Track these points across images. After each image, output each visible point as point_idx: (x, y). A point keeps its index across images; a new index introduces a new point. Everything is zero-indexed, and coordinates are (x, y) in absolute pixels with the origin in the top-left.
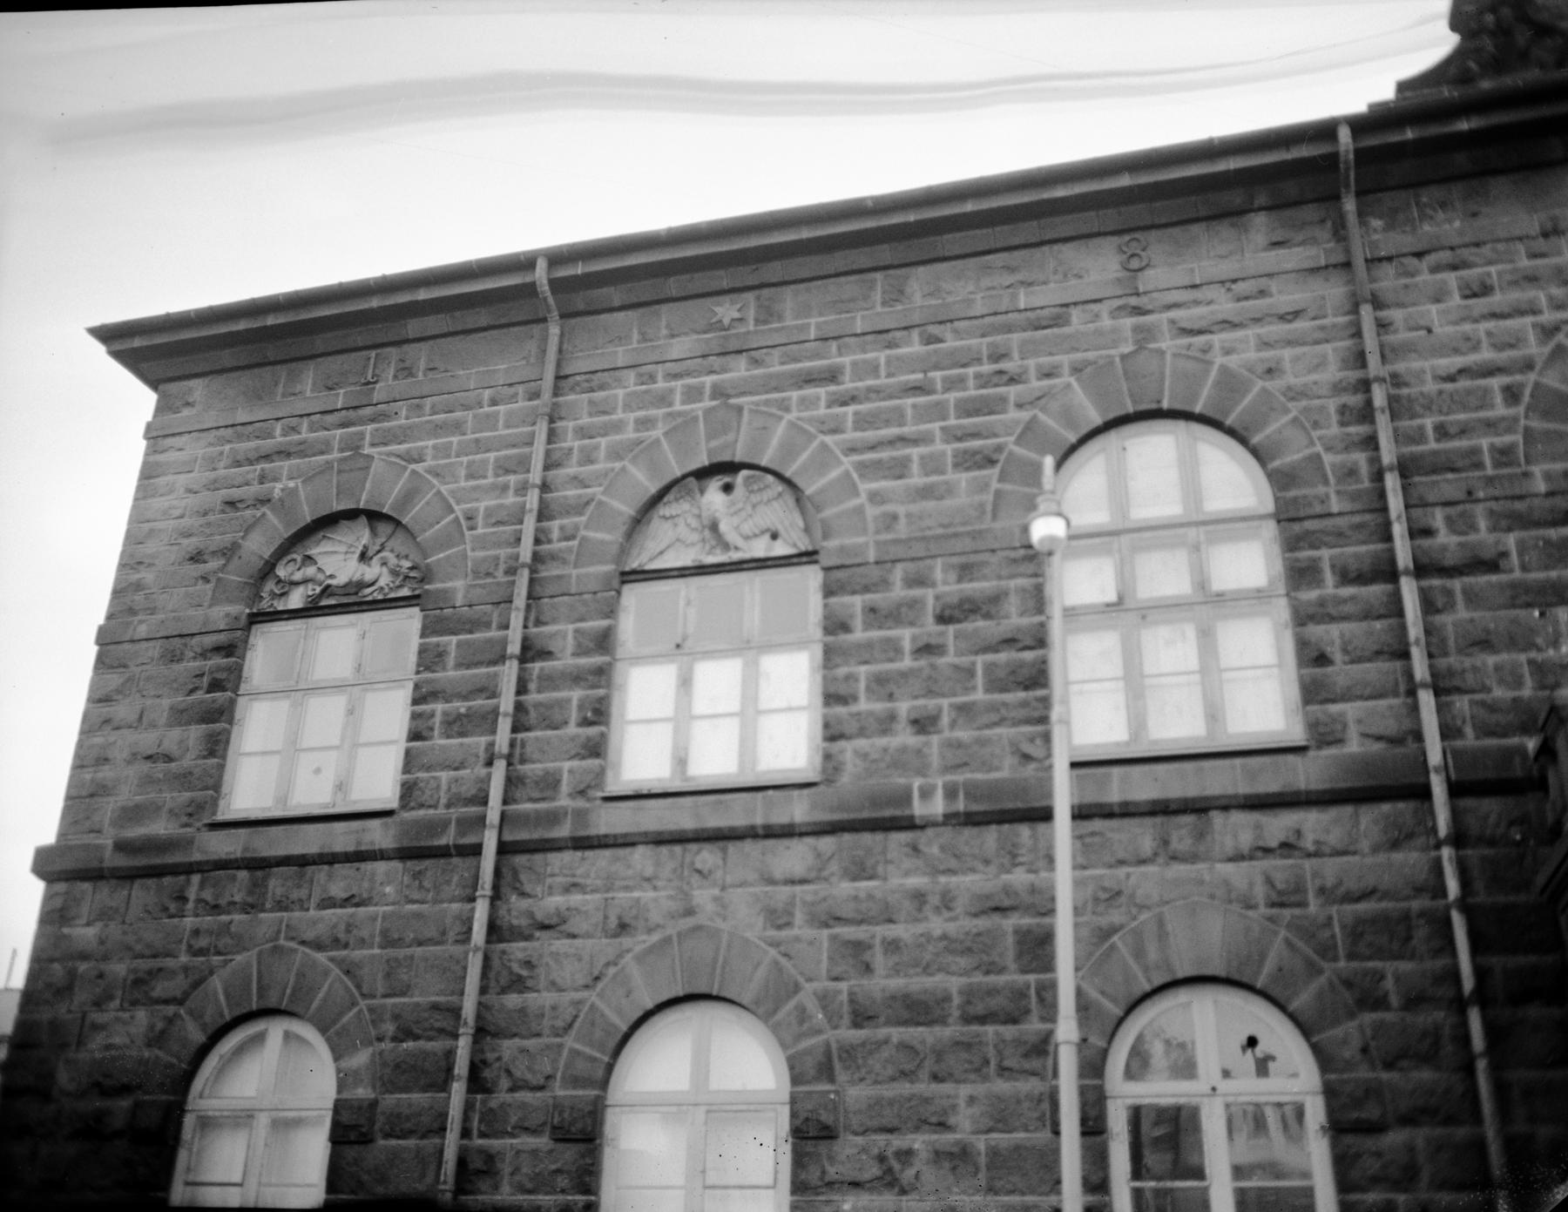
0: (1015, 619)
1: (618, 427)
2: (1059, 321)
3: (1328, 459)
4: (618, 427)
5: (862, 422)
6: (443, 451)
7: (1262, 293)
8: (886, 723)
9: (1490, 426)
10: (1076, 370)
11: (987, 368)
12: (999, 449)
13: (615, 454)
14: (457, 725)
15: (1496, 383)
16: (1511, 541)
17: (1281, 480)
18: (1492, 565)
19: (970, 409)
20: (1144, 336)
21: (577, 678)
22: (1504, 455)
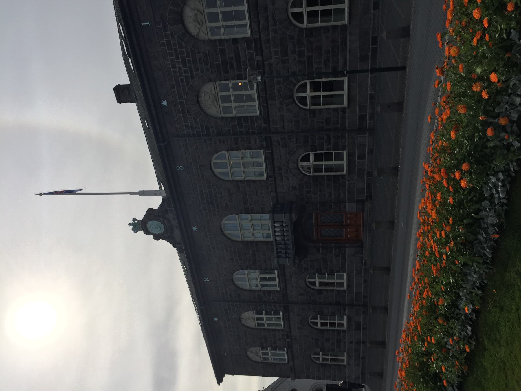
17: (242, 269)
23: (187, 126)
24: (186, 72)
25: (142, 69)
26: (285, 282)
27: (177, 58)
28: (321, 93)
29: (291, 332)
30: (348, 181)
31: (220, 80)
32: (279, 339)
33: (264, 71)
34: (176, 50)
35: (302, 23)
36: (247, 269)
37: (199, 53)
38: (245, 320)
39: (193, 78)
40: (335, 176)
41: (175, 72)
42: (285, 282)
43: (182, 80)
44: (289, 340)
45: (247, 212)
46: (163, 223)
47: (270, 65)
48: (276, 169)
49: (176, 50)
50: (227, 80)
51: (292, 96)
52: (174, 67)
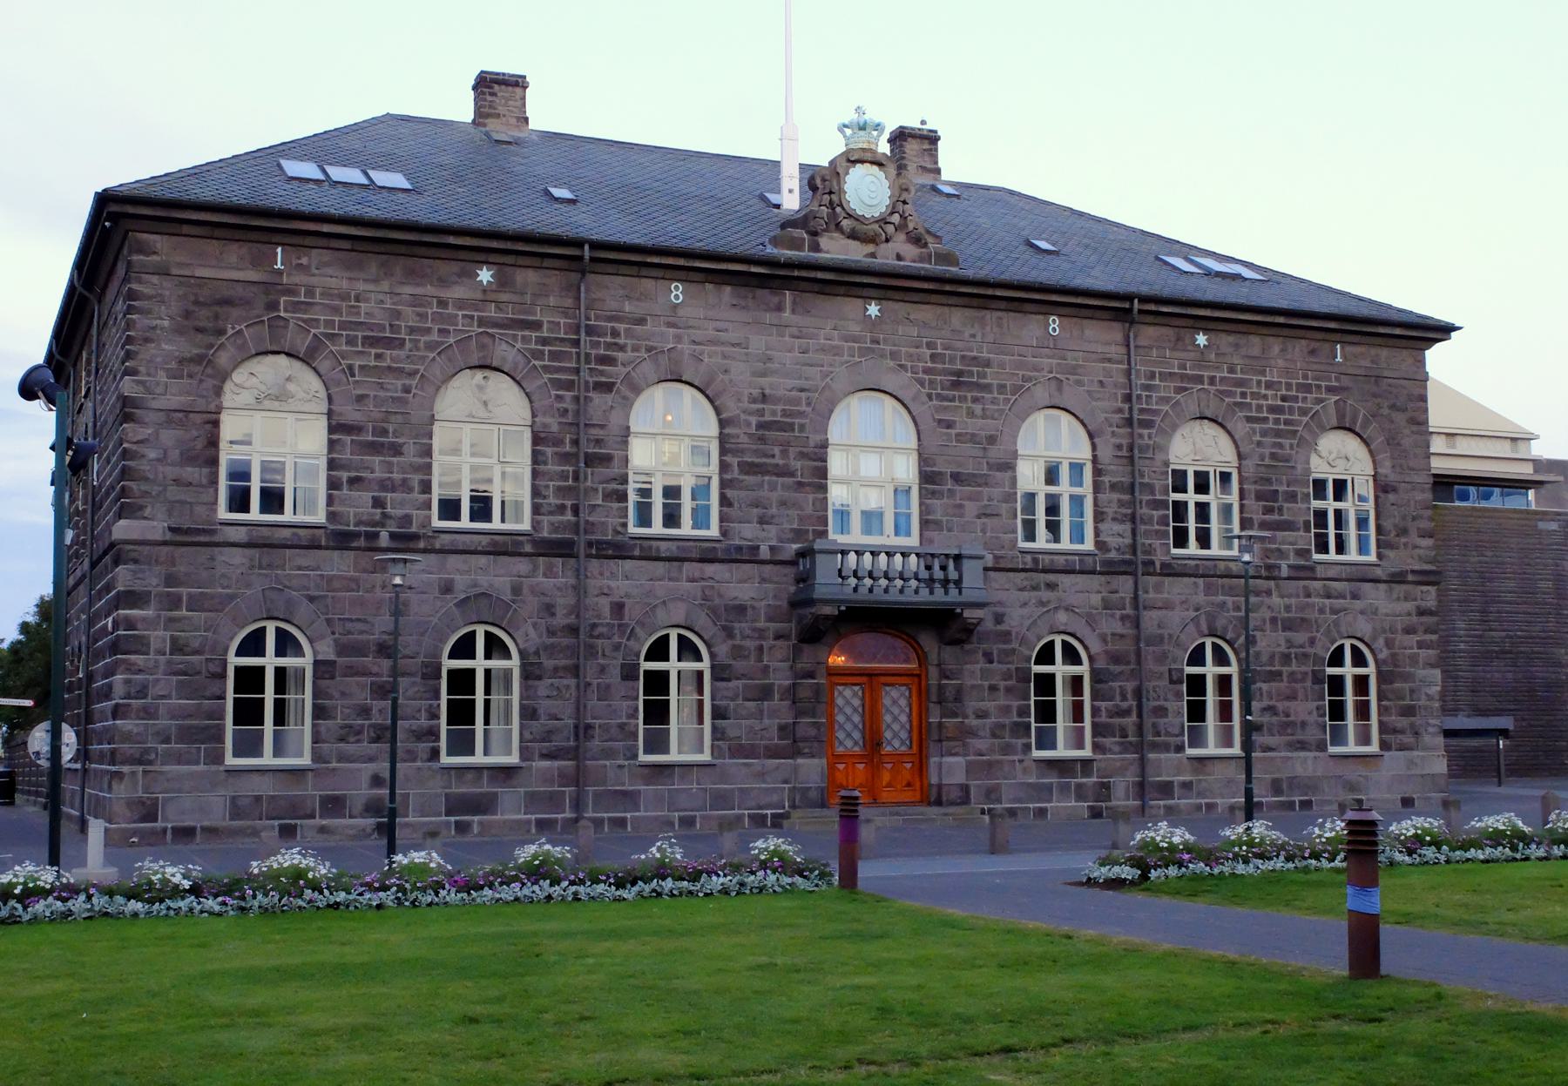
0: (615, 470)
1: (428, 331)
2: (641, 321)
3: (743, 416)
4: (428, 331)
5: (554, 356)
6: (329, 323)
7: (726, 330)
8: (561, 509)
9: (801, 414)
10: (649, 349)
11: (609, 339)
12: (613, 384)
13: (430, 346)
14: (353, 481)
16: (798, 464)
17: (722, 423)
18: (792, 475)
20: (678, 339)
21: (418, 469)
23: (1152, 376)
24: (1259, 408)
25: (1281, 320)
26: (669, 559)
27: (1284, 399)
29: (425, 551)
30: (1021, 761)
31: (1241, 482)
32: (378, 503)
33: (1260, 577)
34: (1295, 399)
35: (239, 653)
37: (1291, 447)
38: (480, 388)
39: (1249, 419)
40: (1028, 726)
42: (669, 559)
43: (1243, 395)
44: (384, 540)
45: (928, 477)
46: (883, 221)
47: (1269, 593)
48: (1051, 577)
49: (1295, 399)
50: (1242, 495)
52: (1269, 385)
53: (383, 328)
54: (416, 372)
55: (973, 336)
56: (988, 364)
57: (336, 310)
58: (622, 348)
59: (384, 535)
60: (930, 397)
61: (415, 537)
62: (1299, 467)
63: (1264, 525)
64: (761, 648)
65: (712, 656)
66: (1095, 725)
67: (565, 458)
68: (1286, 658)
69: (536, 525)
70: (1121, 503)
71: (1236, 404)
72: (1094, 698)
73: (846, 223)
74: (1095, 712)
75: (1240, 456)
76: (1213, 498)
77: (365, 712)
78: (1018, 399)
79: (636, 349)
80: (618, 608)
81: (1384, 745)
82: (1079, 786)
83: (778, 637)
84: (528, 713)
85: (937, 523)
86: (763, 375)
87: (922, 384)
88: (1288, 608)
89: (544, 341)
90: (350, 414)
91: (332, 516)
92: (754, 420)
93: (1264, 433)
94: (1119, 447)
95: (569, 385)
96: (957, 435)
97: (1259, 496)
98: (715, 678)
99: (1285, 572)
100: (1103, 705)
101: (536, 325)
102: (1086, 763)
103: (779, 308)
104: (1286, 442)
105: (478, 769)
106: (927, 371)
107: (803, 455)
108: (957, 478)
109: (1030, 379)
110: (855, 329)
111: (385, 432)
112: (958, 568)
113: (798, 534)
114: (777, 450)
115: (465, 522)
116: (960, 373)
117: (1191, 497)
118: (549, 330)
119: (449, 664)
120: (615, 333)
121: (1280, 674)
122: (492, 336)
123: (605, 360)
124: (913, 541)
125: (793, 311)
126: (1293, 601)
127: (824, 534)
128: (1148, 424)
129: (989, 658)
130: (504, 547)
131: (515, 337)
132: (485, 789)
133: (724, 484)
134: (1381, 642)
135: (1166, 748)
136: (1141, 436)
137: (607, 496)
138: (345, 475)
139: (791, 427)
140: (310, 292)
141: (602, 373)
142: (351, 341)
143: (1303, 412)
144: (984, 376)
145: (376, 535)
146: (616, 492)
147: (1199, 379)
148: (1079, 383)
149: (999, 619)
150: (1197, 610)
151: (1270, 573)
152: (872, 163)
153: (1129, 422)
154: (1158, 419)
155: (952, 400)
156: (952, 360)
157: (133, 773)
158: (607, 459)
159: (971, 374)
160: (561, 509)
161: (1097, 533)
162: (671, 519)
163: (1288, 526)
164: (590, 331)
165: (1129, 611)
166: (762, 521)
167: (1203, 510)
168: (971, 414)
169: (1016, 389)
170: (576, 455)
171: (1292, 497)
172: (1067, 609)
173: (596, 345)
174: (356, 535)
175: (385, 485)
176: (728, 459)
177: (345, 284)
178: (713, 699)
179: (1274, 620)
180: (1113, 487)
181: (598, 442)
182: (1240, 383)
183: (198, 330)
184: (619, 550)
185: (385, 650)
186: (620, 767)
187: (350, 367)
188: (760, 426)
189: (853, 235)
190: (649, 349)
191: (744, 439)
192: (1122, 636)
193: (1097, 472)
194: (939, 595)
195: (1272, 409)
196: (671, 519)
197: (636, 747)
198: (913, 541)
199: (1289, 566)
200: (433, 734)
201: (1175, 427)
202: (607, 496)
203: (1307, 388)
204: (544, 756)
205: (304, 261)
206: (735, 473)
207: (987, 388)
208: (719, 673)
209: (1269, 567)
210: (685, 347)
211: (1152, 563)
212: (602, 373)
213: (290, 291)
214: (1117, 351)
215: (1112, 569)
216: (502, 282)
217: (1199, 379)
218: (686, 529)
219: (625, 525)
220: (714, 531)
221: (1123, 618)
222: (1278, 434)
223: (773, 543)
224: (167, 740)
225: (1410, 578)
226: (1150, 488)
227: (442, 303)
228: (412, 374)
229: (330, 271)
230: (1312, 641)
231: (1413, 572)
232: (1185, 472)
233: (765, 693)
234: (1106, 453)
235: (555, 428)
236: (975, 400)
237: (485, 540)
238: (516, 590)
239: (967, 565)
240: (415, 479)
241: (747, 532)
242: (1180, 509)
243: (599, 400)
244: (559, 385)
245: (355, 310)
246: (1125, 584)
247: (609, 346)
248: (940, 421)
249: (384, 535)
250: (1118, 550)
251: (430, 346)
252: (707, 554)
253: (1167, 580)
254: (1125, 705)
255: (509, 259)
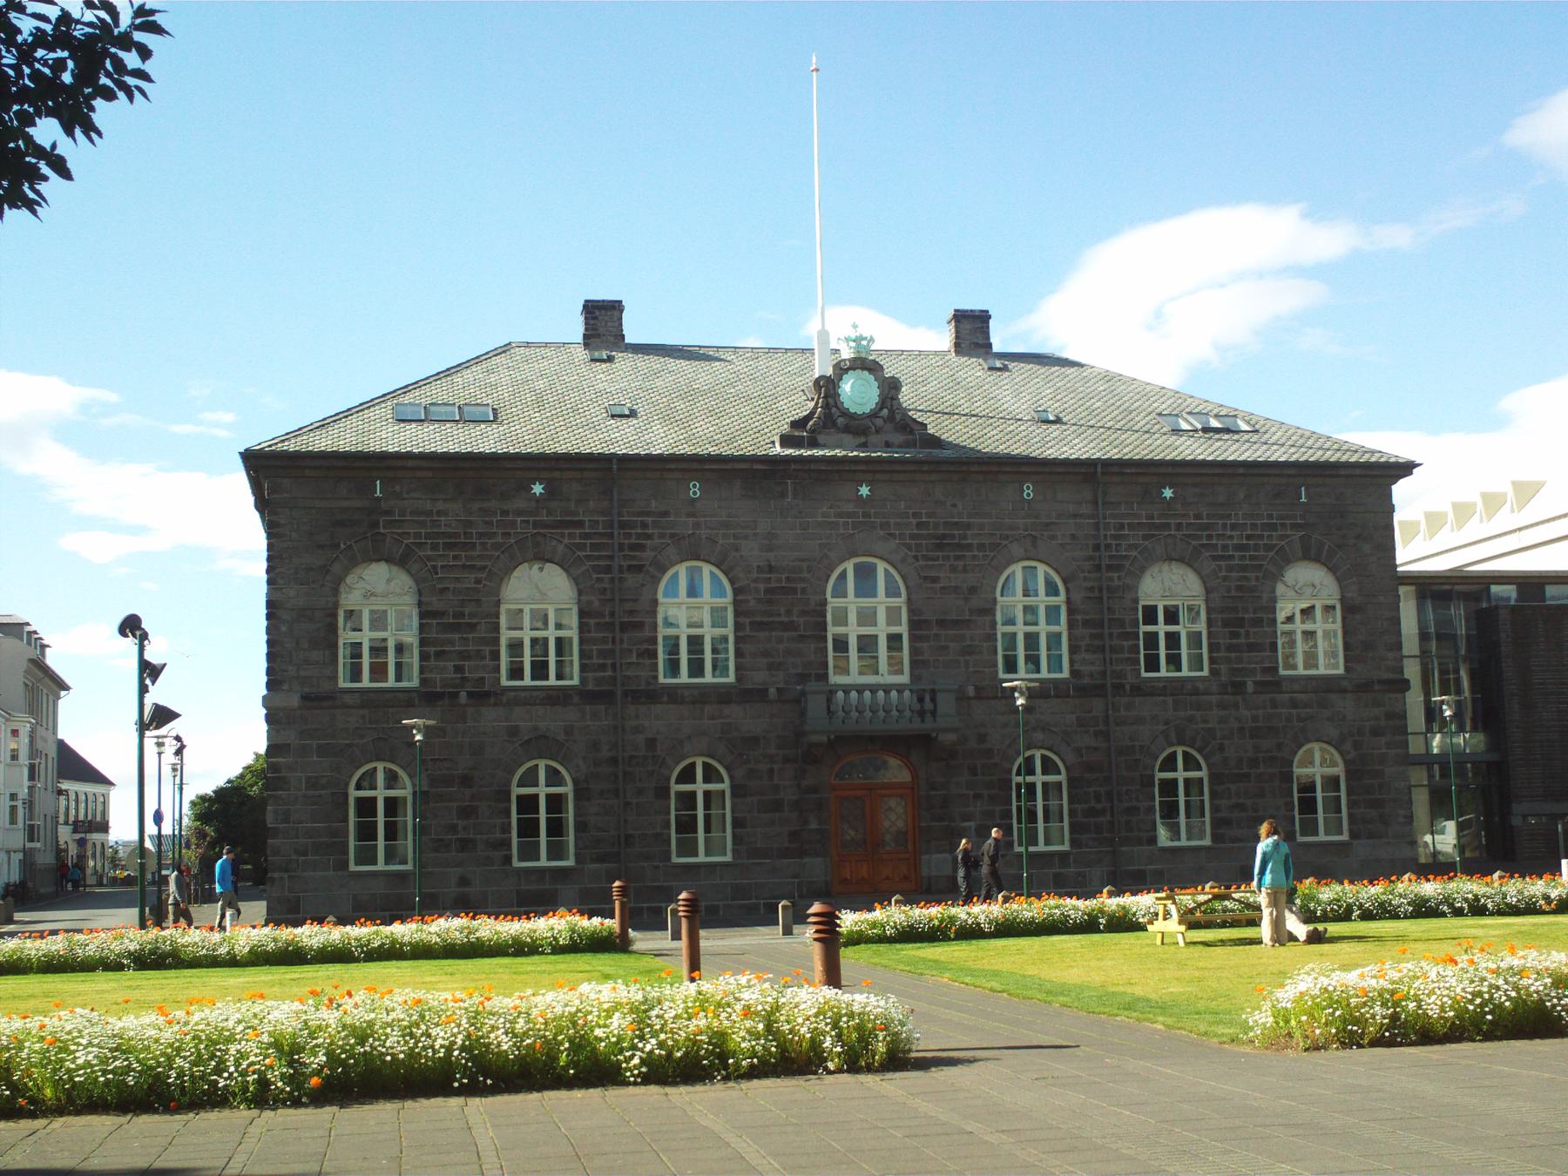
2: (666, 514)
5: (594, 547)
6: (418, 535)
8: (603, 667)
9: (803, 580)
13: (497, 546)
14: (439, 655)
15: (805, 565)
17: (736, 592)
18: (796, 629)
19: (633, 547)
20: (697, 525)
22: (804, 591)
23: (1122, 527)
24: (1225, 547)
27: (1249, 537)
28: (1182, 799)
36: (736, 603)
39: (1215, 558)
41: (1224, 525)
43: (1210, 537)
45: (914, 625)
46: (874, 414)
50: (1210, 623)
51: (1180, 743)
52: (1233, 527)
53: (457, 535)
54: (484, 568)
55: (954, 505)
56: (968, 526)
57: (422, 524)
58: (649, 537)
59: (463, 695)
60: (916, 557)
61: (487, 694)
62: (1265, 596)
63: (1230, 648)
64: (771, 771)
65: (732, 778)
66: (1072, 825)
67: (609, 626)
68: (1254, 762)
69: (583, 680)
70: (1092, 636)
71: (1203, 546)
72: (1071, 802)
73: (840, 421)
74: (1072, 813)
75: (1208, 591)
76: (1182, 629)
77: (453, 829)
78: (996, 556)
79: (662, 536)
80: (651, 743)
81: (1353, 835)
82: (1056, 876)
83: (787, 760)
84: (581, 827)
85: (923, 662)
86: (771, 550)
87: (910, 549)
88: (1255, 719)
89: (586, 536)
90: (436, 604)
91: (423, 681)
92: (762, 586)
93: (1230, 569)
94: (1091, 589)
95: (608, 569)
96: (943, 588)
97: (1226, 624)
98: (733, 795)
99: (1250, 687)
100: (1079, 807)
101: (580, 524)
102: (1063, 856)
103: (783, 495)
104: (1252, 575)
105: (542, 871)
106: (913, 537)
107: (804, 613)
108: (942, 623)
109: (1007, 537)
110: (849, 508)
111: (462, 615)
112: (933, 700)
113: (803, 678)
114: (782, 611)
115: (528, 681)
116: (944, 536)
117: (1161, 628)
118: (591, 527)
119: (517, 791)
120: (644, 525)
121: (1247, 776)
122: (544, 535)
123: (633, 547)
124: (904, 679)
125: (795, 496)
126: (1260, 712)
127: (825, 677)
128: (1119, 568)
129: (973, 771)
130: (557, 698)
131: (563, 535)
132: (547, 887)
133: (738, 640)
134: (1348, 746)
135: (1139, 842)
136: (1111, 579)
137: (640, 655)
138: (433, 649)
139: (794, 591)
140: (402, 513)
141: (634, 558)
142: (434, 547)
143: (1269, 548)
144: (965, 537)
145: (456, 695)
146: (647, 650)
147: (1166, 526)
148: (1053, 537)
149: (982, 738)
150: (1167, 723)
151: (1238, 688)
152: (863, 369)
153: (1098, 568)
154: (1127, 564)
155: (937, 559)
156: (936, 525)
157: (282, 878)
158: (640, 626)
159: (953, 537)
160: (603, 667)
161: (1072, 662)
162: (697, 668)
163: (1252, 647)
164: (623, 525)
165: (1102, 727)
166: (770, 667)
167: (1173, 639)
168: (954, 569)
169: (994, 546)
170: (613, 624)
171: (1258, 622)
172: (1043, 729)
173: (628, 536)
174: (440, 696)
175: (464, 656)
176: (741, 620)
177: (428, 506)
178: (733, 812)
179: (1241, 729)
180: (1086, 623)
181: (632, 612)
182: (1207, 527)
183: (320, 547)
184: (653, 695)
185: (466, 781)
186: (657, 867)
187: (434, 567)
188: (767, 591)
189: (847, 429)
190: (672, 536)
191: (752, 603)
192: (1096, 749)
193: (1070, 612)
194: (917, 726)
195: (1239, 547)
196: (697, 668)
197: (669, 852)
198: (904, 679)
199: (1255, 683)
200: (507, 844)
201: (1143, 570)
202: (640, 655)
203: (1273, 527)
204: (594, 860)
205: (398, 488)
206: (748, 631)
207: (969, 547)
208: (736, 790)
209: (1233, 684)
210: (704, 532)
211: (1122, 686)
212: (634, 558)
213: (389, 513)
214: (1086, 509)
215: (1083, 691)
216: (551, 491)
217: (1166, 526)
218: (708, 678)
219: (656, 677)
220: (731, 678)
221: (1096, 734)
222: (1243, 568)
223: (782, 685)
224: (305, 854)
225: (1377, 687)
226: (1122, 623)
227: (505, 513)
228: (483, 568)
229: (414, 495)
230: (1279, 746)
231: (1379, 682)
232: (1155, 607)
233: (777, 806)
234: (1077, 597)
235: (597, 603)
236: (958, 558)
237: (542, 694)
238: (569, 731)
239: (940, 697)
240: (487, 649)
241: (758, 677)
242: (1152, 639)
243: (631, 580)
244: (596, 569)
245: (436, 523)
246: (1098, 705)
247: (639, 536)
248: (925, 578)
249: (463, 695)
250: (1091, 675)
251: (497, 546)
252: (722, 695)
253: (1137, 699)
254: (1099, 806)
255: (557, 474)
